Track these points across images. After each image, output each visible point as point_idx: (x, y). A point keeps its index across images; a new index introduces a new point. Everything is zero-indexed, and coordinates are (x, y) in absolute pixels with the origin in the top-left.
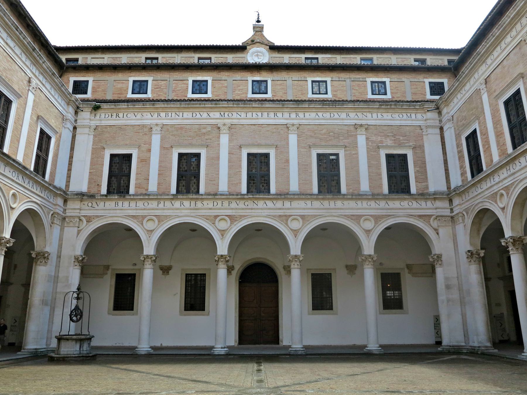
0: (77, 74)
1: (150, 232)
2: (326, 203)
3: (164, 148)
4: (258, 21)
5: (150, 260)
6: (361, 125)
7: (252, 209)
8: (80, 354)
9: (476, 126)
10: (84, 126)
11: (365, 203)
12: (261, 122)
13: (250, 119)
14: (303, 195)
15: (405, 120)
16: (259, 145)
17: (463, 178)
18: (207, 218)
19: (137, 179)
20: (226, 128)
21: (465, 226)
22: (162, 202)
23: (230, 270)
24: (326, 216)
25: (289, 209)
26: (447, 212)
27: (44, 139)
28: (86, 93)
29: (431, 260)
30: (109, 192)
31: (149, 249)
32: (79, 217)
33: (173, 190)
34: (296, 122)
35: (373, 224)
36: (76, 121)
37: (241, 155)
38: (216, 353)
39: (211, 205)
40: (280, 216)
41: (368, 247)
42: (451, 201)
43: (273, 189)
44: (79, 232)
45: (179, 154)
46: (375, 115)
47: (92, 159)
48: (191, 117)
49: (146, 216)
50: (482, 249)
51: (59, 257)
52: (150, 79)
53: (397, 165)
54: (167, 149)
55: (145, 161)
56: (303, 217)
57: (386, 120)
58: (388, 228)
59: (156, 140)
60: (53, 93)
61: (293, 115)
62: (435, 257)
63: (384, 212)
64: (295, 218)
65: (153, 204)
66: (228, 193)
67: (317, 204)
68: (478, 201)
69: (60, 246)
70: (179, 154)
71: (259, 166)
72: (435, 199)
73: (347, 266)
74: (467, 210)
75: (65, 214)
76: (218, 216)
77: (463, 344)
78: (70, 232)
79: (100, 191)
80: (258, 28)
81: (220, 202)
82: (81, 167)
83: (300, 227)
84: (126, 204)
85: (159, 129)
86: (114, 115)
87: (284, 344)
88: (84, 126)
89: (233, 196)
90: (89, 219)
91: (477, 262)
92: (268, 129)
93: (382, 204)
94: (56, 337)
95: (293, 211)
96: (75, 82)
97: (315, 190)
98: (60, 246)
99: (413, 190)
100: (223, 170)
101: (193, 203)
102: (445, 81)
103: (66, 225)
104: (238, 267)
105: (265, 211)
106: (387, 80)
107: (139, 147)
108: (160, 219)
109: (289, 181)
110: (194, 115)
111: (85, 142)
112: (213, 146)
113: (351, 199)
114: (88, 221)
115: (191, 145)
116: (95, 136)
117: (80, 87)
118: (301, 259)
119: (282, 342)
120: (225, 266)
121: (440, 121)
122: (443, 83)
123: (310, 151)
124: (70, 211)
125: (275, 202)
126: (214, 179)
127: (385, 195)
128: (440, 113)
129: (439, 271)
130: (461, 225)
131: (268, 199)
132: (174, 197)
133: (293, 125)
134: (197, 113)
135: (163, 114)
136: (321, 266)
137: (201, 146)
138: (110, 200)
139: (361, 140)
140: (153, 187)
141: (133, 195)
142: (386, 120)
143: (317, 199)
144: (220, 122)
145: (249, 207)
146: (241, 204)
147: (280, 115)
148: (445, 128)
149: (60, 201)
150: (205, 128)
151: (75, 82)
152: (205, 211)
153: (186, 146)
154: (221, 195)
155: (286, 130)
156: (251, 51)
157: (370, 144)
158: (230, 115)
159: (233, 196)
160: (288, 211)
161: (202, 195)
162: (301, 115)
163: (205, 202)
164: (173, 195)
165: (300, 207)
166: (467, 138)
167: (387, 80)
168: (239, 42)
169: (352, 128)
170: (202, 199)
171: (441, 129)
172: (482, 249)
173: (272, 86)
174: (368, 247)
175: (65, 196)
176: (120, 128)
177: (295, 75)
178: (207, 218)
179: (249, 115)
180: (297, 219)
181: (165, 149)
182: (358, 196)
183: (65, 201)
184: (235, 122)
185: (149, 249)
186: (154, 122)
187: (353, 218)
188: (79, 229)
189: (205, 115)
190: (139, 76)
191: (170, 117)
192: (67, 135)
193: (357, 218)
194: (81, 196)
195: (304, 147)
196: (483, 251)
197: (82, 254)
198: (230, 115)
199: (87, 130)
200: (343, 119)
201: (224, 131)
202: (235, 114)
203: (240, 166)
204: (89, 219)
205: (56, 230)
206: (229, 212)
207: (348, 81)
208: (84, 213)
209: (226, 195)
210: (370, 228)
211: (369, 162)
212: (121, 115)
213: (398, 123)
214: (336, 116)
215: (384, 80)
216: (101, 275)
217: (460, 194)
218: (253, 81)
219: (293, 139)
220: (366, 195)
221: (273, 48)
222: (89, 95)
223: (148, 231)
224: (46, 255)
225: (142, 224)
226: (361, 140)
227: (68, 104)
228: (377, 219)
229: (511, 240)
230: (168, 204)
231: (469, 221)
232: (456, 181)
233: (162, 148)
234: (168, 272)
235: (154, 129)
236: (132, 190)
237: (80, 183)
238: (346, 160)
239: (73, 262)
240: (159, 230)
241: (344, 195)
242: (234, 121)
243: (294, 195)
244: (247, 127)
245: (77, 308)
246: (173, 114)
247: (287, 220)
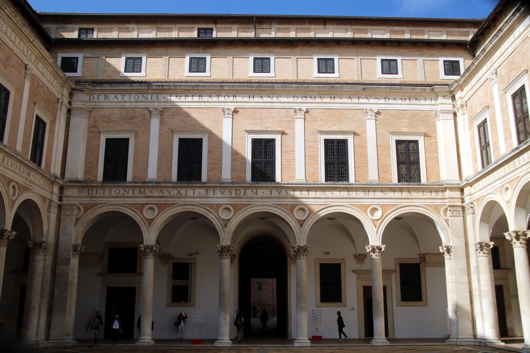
1: (150, 222)
9: (486, 115)
19: (135, 166)
27: (40, 124)
28: (76, 71)
29: (441, 251)
42: (462, 190)
45: (179, 139)
58: (398, 218)
62: (445, 249)
66: (231, 181)
70: (179, 139)
82: (75, 151)
96: (63, 59)
106: (399, 59)
117: (69, 65)
120: (229, 257)
128: (453, 98)
140: (152, 174)
148: (458, 114)
151: (63, 59)
159: (235, 185)
161: (204, 183)
166: (479, 127)
171: (455, 114)
183: (61, 188)
196: (493, 243)
217: (471, 185)
222: (79, 74)
225: (142, 213)
229: (514, 235)
237: (77, 170)
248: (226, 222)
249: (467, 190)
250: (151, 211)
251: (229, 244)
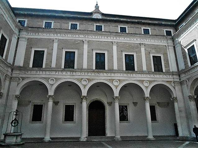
0: (21, 18)
2: (129, 75)
3: (59, 49)
4: (97, 5)
5: (51, 98)
6: (142, 44)
7: (97, 76)
8: (16, 143)
10: (23, 38)
11: (145, 75)
12: (101, 40)
13: (96, 39)
14: (119, 71)
15: (159, 43)
16: (101, 50)
17: (186, 66)
18: (78, 79)
20: (87, 42)
21: (187, 86)
22: (58, 72)
24: (129, 80)
25: (113, 77)
26: (178, 80)
30: (33, 66)
31: (51, 93)
32: (18, 77)
33: (63, 67)
34: (116, 41)
35: (149, 84)
36: (19, 35)
37: (93, 53)
38: (82, 140)
39: (79, 74)
41: (147, 94)
43: (106, 68)
44: (18, 84)
45: (66, 51)
46: (147, 40)
47: (26, 52)
48: (71, 36)
49: (50, 78)
50: (195, 95)
51: (8, 95)
52: (53, 22)
53: (157, 60)
54: (60, 49)
55: (50, 54)
56: (119, 80)
57: (152, 42)
59: (55, 45)
60: (9, 19)
61: (115, 38)
63: (153, 79)
64: (117, 80)
65: (54, 73)
67: (125, 75)
68: (195, 75)
69: (9, 90)
70: (66, 51)
71: (100, 58)
72: (173, 75)
73: (133, 103)
74: (188, 79)
75: (12, 75)
76: (83, 79)
77: (189, 136)
78: (14, 84)
79: (29, 66)
80: (97, 7)
83: (118, 85)
84: (41, 73)
85: (57, 40)
86: (37, 34)
87: (108, 136)
88: (23, 38)
89: (89, 70)
90: (23, 79)
91: (193, 101)
92: (104, 43)
93: (152, 76)
94: (4, 134)
95: (115, 77)
97: (124, 69)
98: (9, 90)
99: (164, 71)
100: (85, 59)
101: (71, 73)
102: (172, 30)
103: (12, 81)
104: (89, 101)
107: (48, 48)
108: (57, 79)
109: (113, 65)
110: (73, 36)
111: (23, 45)
112: (81, 49)
113: (140, 73)
114: (23, 80)
115: (72, 48)
116: (28, 42)
119: (107, 135)
121: (174, 44)
122: (171, 31)
123: (122, 53)
124: (14, 74)
126: (81, 63)
127: (153, 72)
129: (176, 104)
130: (186, 85)
132: (62, 71)
133: (115, 42)
134: (74, 35)
135: (59, 35)
136: (124, 103)
137: (76, 49)
138: (34, 70)
139: (143, 49)
140: (53, 65)
141: (45, 68)
142: (152, 42)
143: (125, 73)
144: (84, 39)
145: (96, 75)
147: (109, 38)
149: (10, 70)
150: (77, 41)
152: (77, 76)
153: (68, 49)
154: (84, 70)
155: (112, 44)
156: (94, 15)
157: (146, 51)
158: (88, 37)
160: (113, 78)
161: (76, 69)
162: (118, 38)
163: (77, 73)
164: (63, 69)
165: (118, 76)
167: (150, 29)
168: (90, 11)
169: (139, 45)
170: (76, 71)
171: (174, 47)
172: (195, 95)
173: (104, 28)
174: (147, 94)
175: (13, 67)
176: (40, 39)
177: (114, 24)
178: (78, 79)
179: (96, 37)
180: (117, 81)
181: (60, 49)
182: (141, 72)
183: (12, 70)
184: (90, 39)
185: (51, 93)
186: (55, 38)
187: (140, 81)
188: (18, 83)
189: (77, 36)
190: (48, 20)
191: (62, 36)
192: (14, 41)
193: (142, 81)
194: (20, 68)
195: (120, 51)
197: (19, 94)
198: (88, 37)
199: (24, 39)
200: (135, 41)
201: (86, 43)
202: (90, 36)
203: (93, 58)
204: (23, 79)
205: (7, 83)
207: (134, 28)
208: (21, 76)
210: (147, 86)
211: (146, 59)
212: (40, 34)
213: (157, 44)
214: (132, 40)
215: (148, 28)
216: (27, 105)
217: (185, 73)
218: (96, 26)
219: (115, 48)
220: (146, 72)
221: (103, 14)
223: (51, 84)
224: (1, 94)
225: (48, 81)
226: (143, 49)
227: (16, 27)
228: (150, 82)
230: (60, 73)
231: (190, 83)
232: (182, 66)
233: (58, 49)
234: (57, 105)
235: (54, 41)
236: (44, 66)
238: (137, 57)
239: (14, 98)
240: (55, 85)
241: (137, 72)
242: (90, 39)
243: (116, 71)
244: (95, 42)
245: (15, 119)
246: (64, 35)
247: (113, 81)
248: (85, 86)
249: (183, 75)
250: (52, 81)
251: (86, 95)
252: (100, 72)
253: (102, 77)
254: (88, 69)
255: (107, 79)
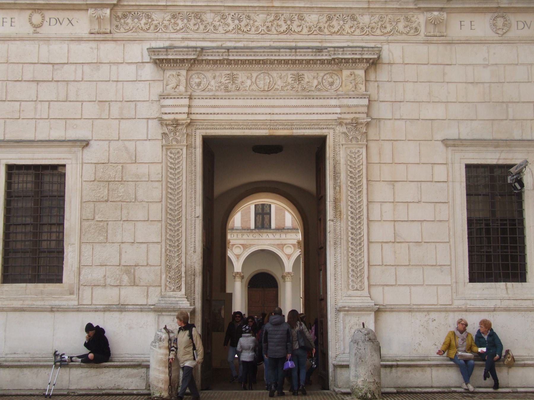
23: (242, 277)
40: (278, 245)
43: (273, 226)
76: (235, 244)
81: (235, 235)
105: (268, 241)
118: (292, 275)
125: (274, 234)
131: (270, 232)
145: (256, 238)
146: (251, 237)
160: (283, 241)
206: (242, 242)
209: (240, 230)
247: (283, 248)
252: (261, 232)
253: (265, 241)
254: (243, 229)
255: (274, 245)
